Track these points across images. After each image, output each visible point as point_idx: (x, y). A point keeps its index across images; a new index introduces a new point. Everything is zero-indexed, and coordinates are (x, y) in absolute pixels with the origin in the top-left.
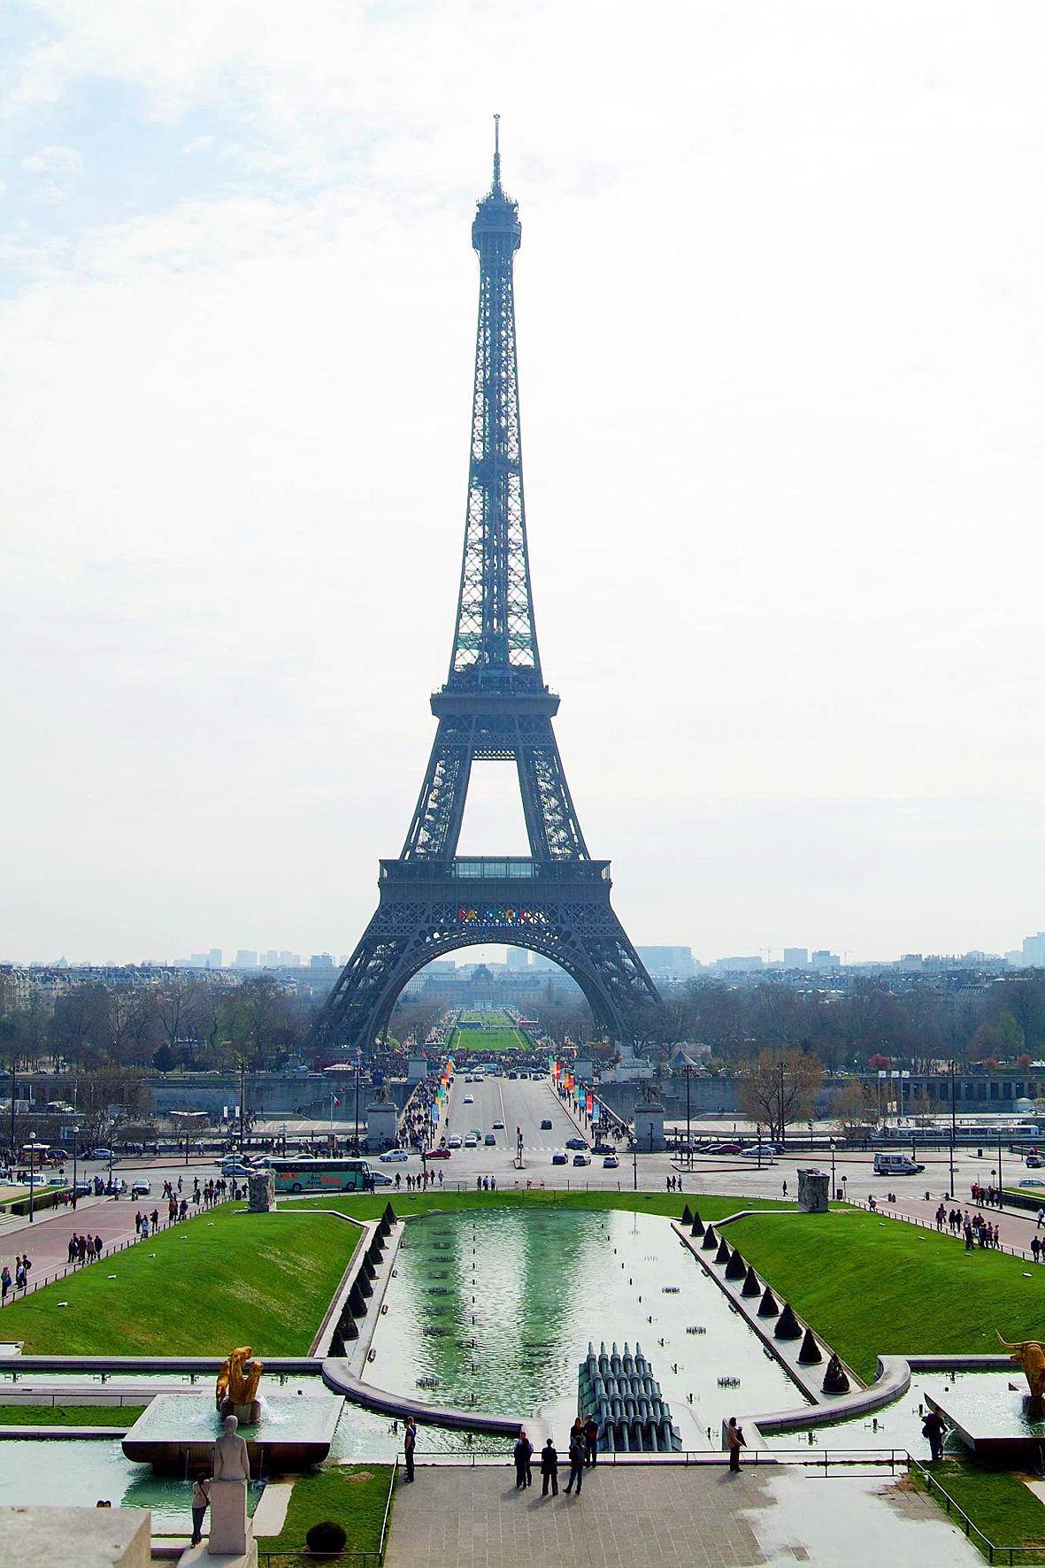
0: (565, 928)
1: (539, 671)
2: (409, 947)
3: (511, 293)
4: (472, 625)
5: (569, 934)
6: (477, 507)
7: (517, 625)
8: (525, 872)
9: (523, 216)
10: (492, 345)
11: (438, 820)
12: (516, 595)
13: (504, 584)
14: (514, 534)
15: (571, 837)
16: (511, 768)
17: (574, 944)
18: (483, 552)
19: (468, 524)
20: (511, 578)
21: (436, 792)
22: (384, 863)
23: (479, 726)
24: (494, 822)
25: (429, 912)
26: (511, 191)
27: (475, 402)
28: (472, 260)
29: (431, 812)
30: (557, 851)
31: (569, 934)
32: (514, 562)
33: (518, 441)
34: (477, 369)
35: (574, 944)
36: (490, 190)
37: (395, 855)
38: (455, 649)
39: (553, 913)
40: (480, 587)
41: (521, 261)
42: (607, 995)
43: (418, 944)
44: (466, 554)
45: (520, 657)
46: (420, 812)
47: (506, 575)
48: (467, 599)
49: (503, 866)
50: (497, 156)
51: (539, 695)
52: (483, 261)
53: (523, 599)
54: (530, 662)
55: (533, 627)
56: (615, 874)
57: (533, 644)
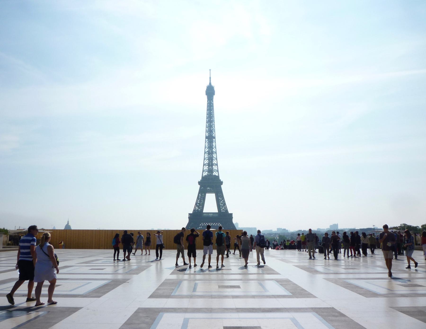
3: (213, 104)
4: (206, 168)
6: (207, 145)
7: (215, 168)
8: (217, 215)
11: (200, 205)
12: (214, 162)
13: (212, 160)
24: (211, 206)
26: (213, 84)
28: (205, 97)
29: (199, 204)
32: (214, 155)
36: (208, 84)
38: (203, 172)
41: (215, 97)
45: (215, 174)
46: (196, 204)
48: (205, 163)
50: (210, 78)
52: (208, 98)
54: (217, 175)
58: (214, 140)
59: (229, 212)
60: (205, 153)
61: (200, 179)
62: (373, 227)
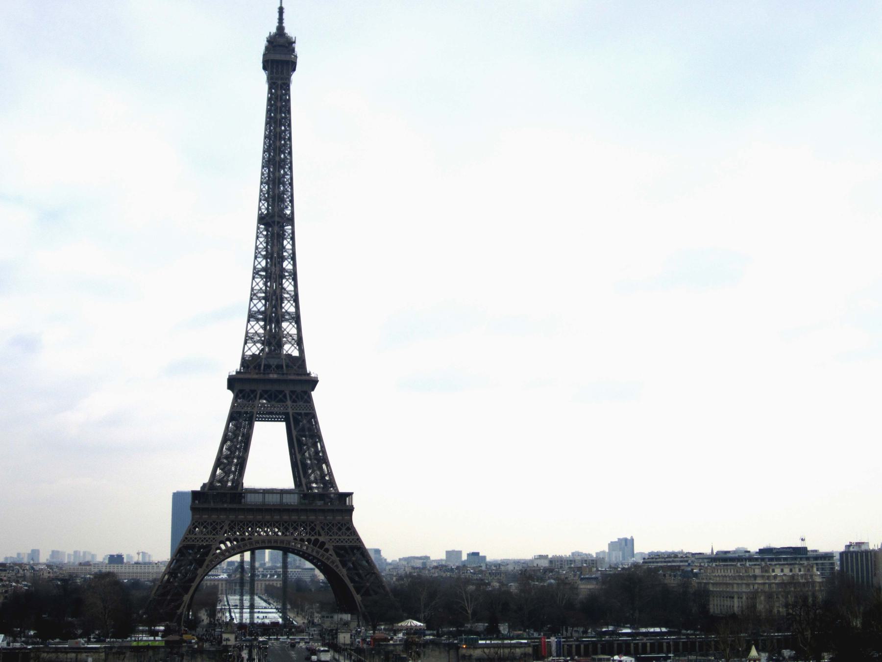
0: (321, 539)
1: (304, 361)
3: (289, 100)
4: (258, 327)
5: (323, 544)
7: (288, 328)
8: (293, 500)
9: (298, 48)
10: (275, 136)
12: (288, 307)
14: (287, 265)
15: (323, 476)
16: (280, 428)
17: (327, 550)
18: (266, 277)
19: (256, 257)
20: (286, 295)
21: (229, 443)
22: (195, 494)
23: (261, 397)
24: (269, 464)
25: (226, 528)
26: (289, 30)
27: (262, 174)
29: (227, 457)
30: (314, 485)
32: (288, 285)
33: (292, 201)
34: (264, 152)
35: (327, 550)
36: (274, 30)
39: (313, 529)
40: (263, 301)
41: (297, 80)
42: (351, 586)
44: (254, 278)
45: (290, 349)
47: (281, 293)
48: (255, 309)
49: (278, 496)
50: (281, 10)
51: (304, 378)
53: (292, 310)
54: (296, 353)
55: (299, 329)
56: (356, 502)
57: (299, 342)
58: (288, 228)
59: (342, 488)
60: (256, 272)
61: (234, 366)
62: (799, 544)
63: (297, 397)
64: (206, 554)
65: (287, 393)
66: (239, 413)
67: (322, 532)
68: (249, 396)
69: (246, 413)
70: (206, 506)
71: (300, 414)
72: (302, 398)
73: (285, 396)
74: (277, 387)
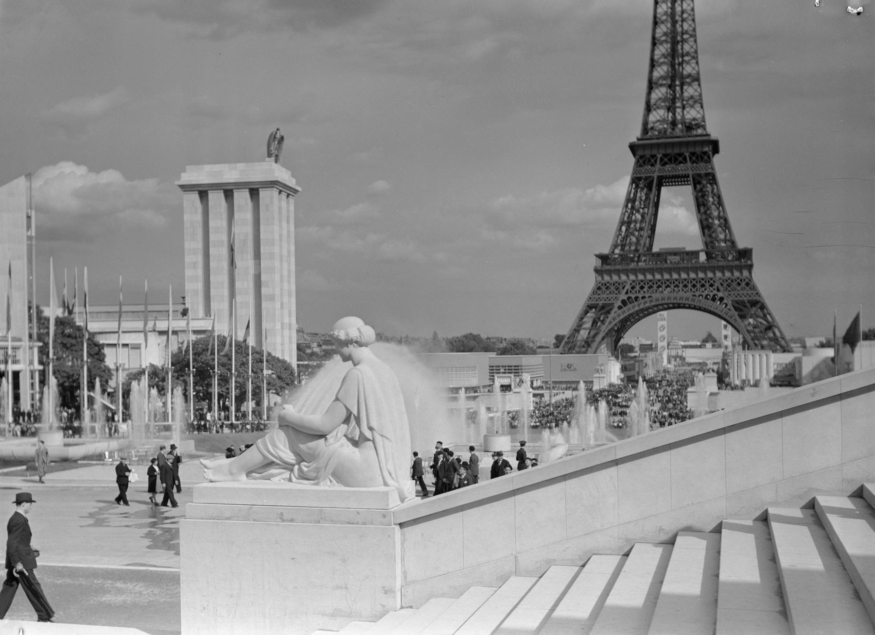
0: (720, 295)
2: (615, 309)
25: (628, 287)
31: (721, 299)
37: (606, 251)
43: (620, 308)
59: (741, 245)
61: (635, 134)
63: (697, 158)
64: (609, 312)
65: (687, 155)
66: (639, 179)
67: (721, 288)
68: (649, 161)
69: (646, 178)
70: (608, 267)
71: (699, 175)
72: (702, 158)
73: (685, 159)
74: (677, 151)
